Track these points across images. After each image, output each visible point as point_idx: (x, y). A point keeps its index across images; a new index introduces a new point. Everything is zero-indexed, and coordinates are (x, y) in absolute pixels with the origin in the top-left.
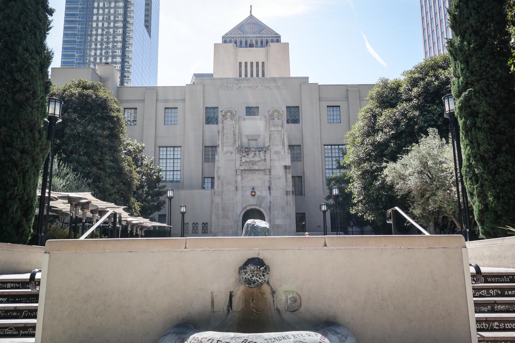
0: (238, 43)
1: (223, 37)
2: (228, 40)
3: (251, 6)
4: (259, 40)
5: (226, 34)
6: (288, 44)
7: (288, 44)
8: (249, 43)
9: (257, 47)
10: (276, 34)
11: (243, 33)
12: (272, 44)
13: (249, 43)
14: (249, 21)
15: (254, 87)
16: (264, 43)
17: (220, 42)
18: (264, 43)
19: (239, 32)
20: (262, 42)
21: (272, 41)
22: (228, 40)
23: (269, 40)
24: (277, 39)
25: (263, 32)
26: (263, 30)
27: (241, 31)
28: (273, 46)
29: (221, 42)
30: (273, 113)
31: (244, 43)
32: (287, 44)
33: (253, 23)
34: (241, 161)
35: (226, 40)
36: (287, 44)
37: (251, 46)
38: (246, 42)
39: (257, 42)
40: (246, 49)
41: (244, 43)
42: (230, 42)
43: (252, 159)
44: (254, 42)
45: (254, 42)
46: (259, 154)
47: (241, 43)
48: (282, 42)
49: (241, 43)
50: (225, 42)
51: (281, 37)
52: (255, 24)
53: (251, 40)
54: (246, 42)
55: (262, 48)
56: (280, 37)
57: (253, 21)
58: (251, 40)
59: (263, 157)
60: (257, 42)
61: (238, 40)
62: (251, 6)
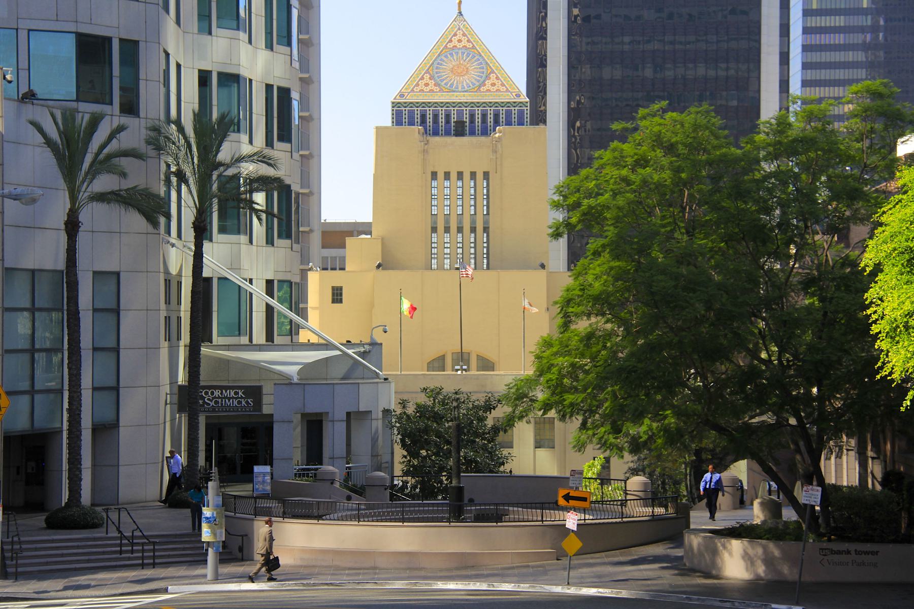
1: (394, 104)
2: (405, 111)
9: (472, 133)
16: (490, 119)
18: (490, 119)
22: (405, 111)
23: (502, 111)
26: (488, 77)
29: (389, 124)
31: (442, 120)
38: (448, 116)
39: (472, 116)
41: (442, 120)
42: (411, 123)
50: (398, 119)
53: (460, 113)
54: (448, 116)
55: (483, 138)
57: (464, 42)
58: (460, 113)
60: (472, 116)
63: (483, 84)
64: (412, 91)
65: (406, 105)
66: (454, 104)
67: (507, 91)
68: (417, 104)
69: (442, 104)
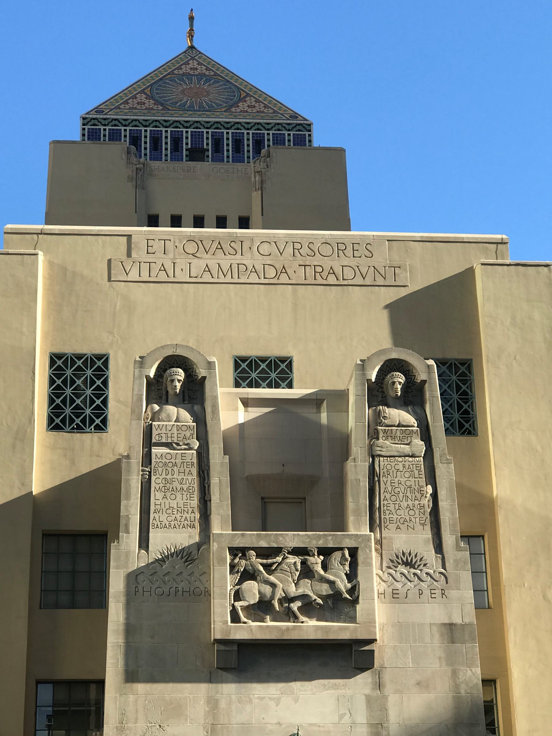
0: (146, 143)
1: (85, 121)
2: (105, 130)
3: (191, 18)
4: (228, 136)
5: (98, 110)
6: (341, 152)
7: (341, 152)
8: (186, 143)
10: (295, 116)
11: (165, 108)
12: (278, 153)
13: (186, 143)
14: (185, 69)
15: (271, 273)
16: (248, 145)
17: (74, 132)
18: (248, 145)
19: (150, 103)
20: (238, 144)
21: (279, 141)
22: (105, 130)
23: (268, 136)
24: (299, 132)
25: (242, 106)
26: (243, 100)
27: (157, 103)
28: (283, 157)
29: (77, 137)
30: (384, 372)
31: (166, 145)
32: (336, 156)
33: (202, 75)
34: (238, 596)
35: (95, 127)
36: (336, 156)
37: (197, 154)
38: (176, 142)
40: (177, 165)
41: (166, 145)
42: (115, 136)
43: (293, 590)
44: (208, 144)
45: (208, 144)
46: (325, 567)
47: (156, 142)
48: (315, 144)
49: (156, 142)
51: (314, 128)
52: (208, 79)
53: (197, 137)
54: (176, 142)
56: (308, 127)
58: (197, 137)
59: (343, 585)
61: (146, 133)
62: (191, 18)
63: (236, 105)
64: (118, 107)
65: (106, 122)
66: (187, 125)
67: (275, 112)
68: (125, 123)
69: (167, 124)
